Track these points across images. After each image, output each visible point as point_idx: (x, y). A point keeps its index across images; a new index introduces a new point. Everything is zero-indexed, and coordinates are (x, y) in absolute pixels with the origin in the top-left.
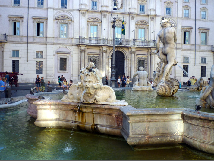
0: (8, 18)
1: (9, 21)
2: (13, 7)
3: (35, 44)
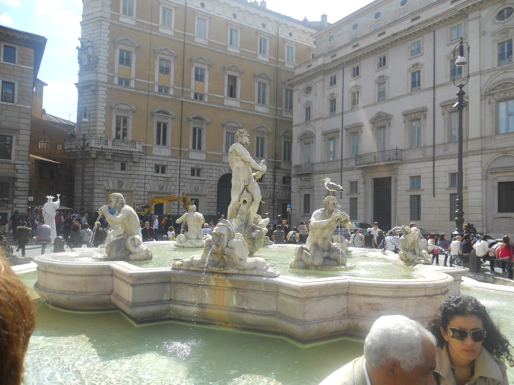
0: (402, 118)
1: (404, 122)
2: (410, 94)
3: (448, 159)
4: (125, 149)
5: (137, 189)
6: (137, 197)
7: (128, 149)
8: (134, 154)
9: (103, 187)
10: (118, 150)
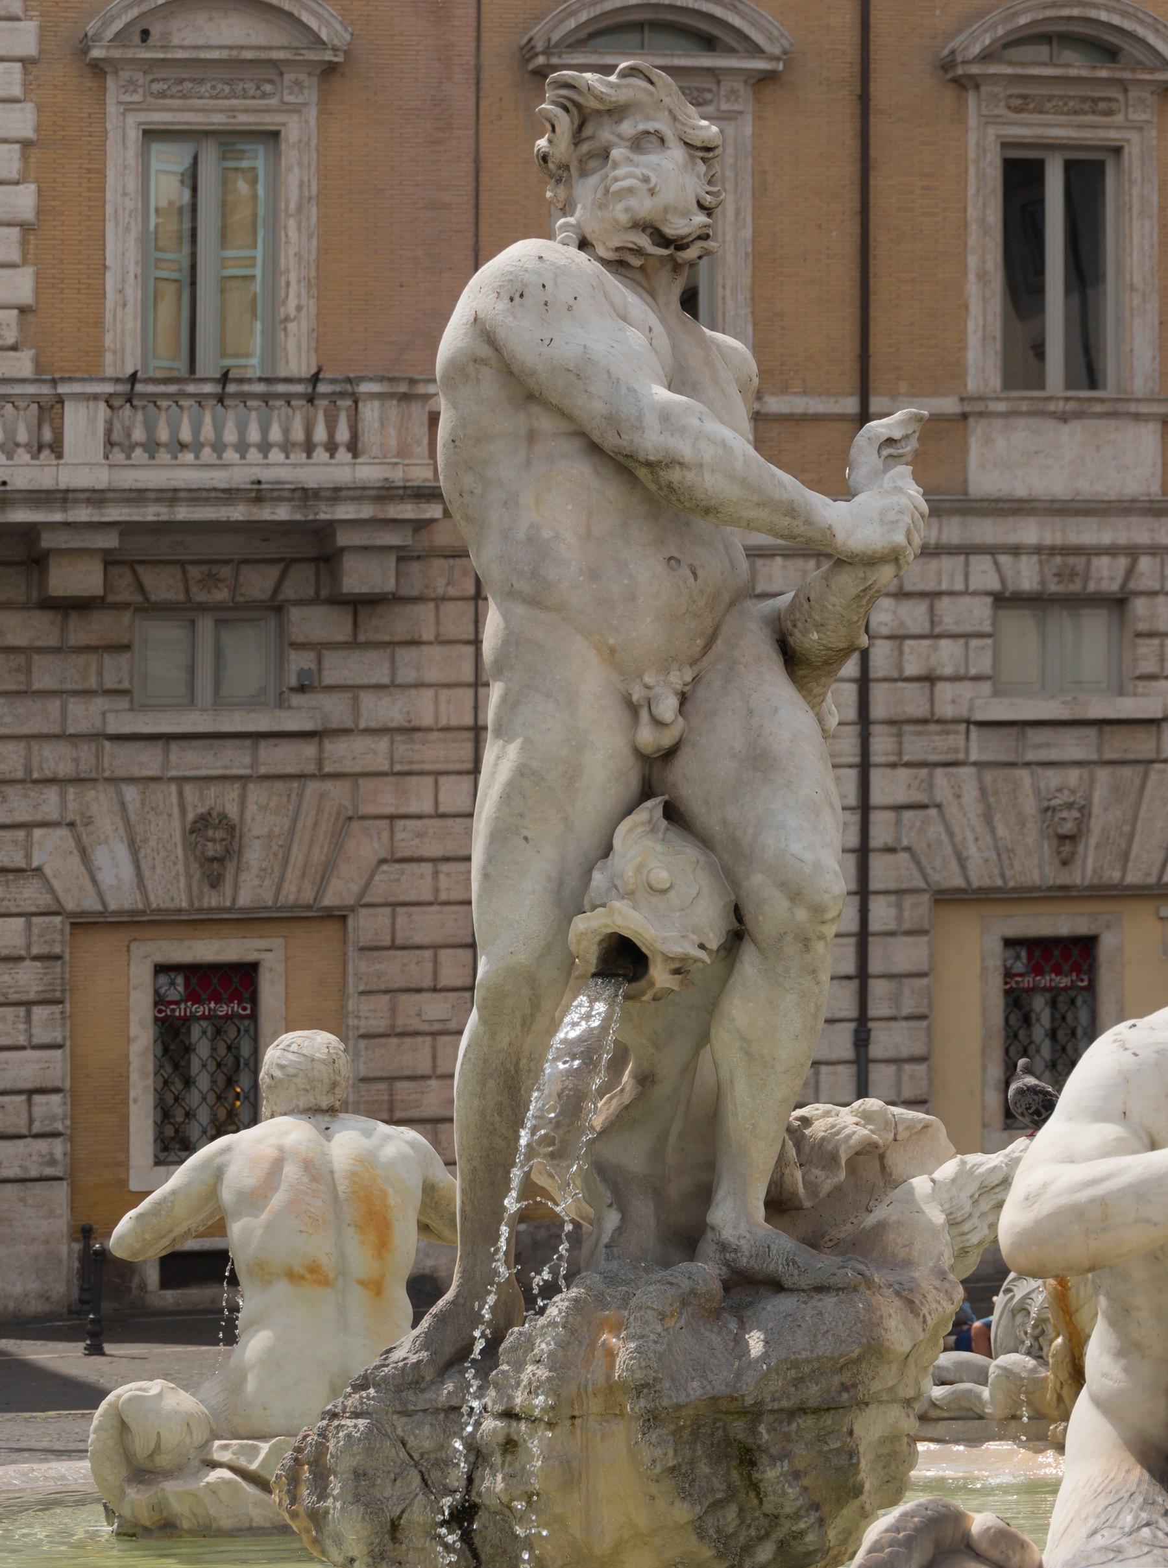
4: (239, 476)
5: (385, 884)
6: (395, 969)
7: (281, 470)
8: (345, 512)
9: (29, 894)
10: (171, 496)
